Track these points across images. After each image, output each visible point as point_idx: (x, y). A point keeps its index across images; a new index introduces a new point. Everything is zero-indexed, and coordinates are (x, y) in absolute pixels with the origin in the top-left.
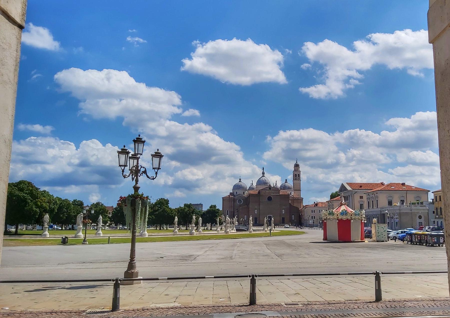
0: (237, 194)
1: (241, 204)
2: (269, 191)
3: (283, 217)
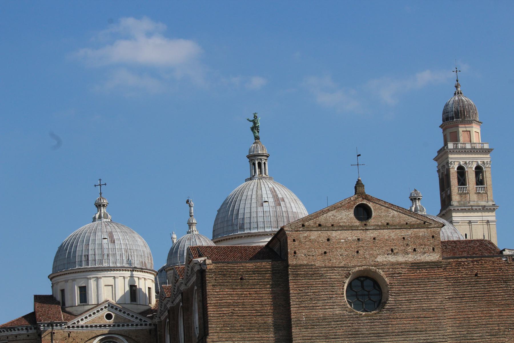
2: (358, 234)
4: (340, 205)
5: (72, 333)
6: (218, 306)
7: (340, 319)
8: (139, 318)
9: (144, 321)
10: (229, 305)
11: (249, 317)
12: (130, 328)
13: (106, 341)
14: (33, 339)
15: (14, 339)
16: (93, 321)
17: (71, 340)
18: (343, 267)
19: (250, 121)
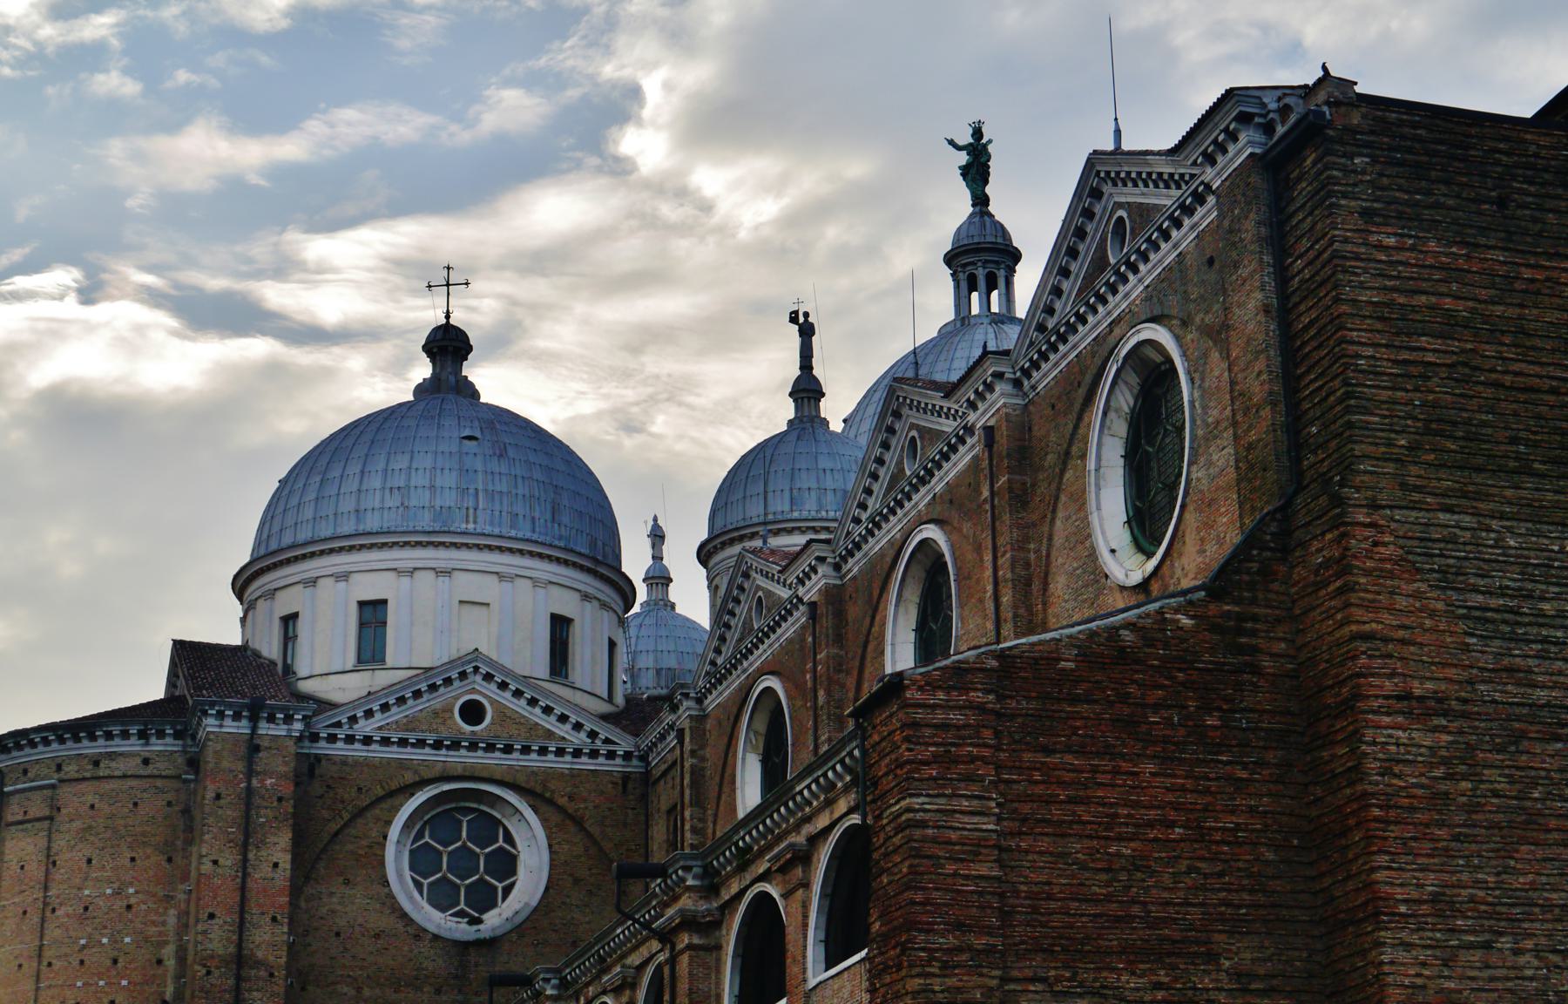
0: (370, 651)
1: (493, 920)
5: (323, 762)
8: (588, 726)
9: (607, 741)
10: (1449, 326)
11: (1551, 398)
13: (453, 805)
14: (165, 777)
15: (88, 775)
16: (410, 724)
17: (317, 788)
19: (959, 148)
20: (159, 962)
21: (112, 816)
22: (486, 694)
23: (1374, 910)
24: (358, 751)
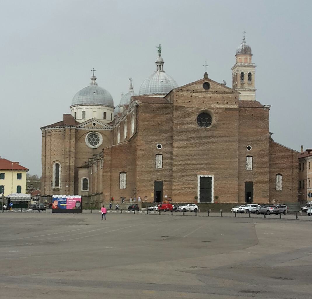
0: (84, 118)
1: (97, 146)
3: (248, 180)
4: (197, 82)
6: (143, 121)
7: (194, 129)
10: (148, 121)
12: (103, 129)
16: (87, 126)
17: (78, 133)
18: (197, 108)
20: (62, 151)
21: (57, 136)
22: (95, 122)
23: (137, 165)
24: (82, 129)
